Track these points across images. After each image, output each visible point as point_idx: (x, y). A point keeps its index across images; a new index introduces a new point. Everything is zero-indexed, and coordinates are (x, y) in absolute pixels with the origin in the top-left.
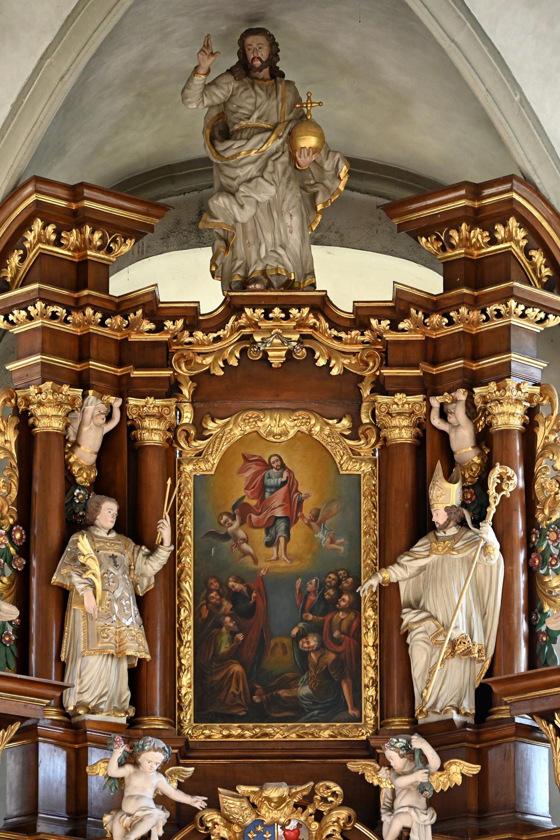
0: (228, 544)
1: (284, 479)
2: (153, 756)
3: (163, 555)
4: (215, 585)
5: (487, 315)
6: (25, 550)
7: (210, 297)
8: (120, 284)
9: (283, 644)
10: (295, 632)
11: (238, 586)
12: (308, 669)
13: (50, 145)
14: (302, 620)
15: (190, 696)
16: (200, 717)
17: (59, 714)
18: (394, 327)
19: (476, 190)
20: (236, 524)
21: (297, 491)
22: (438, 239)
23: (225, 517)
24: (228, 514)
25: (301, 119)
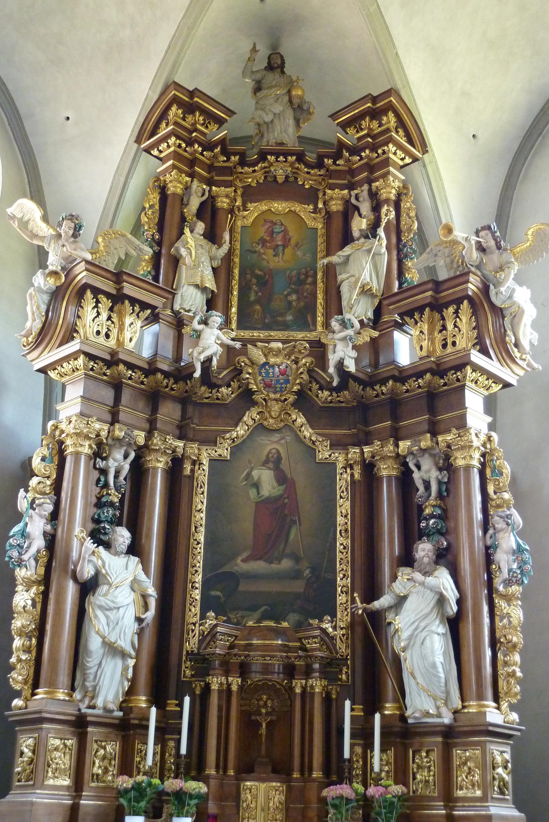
0: (255, 256)
1: (283, 229)
3: (225, 248)
4: (249, 272)
5: (378, 154)
9: (280, 298)
10: (285, 293)
11: (259, 273)
12: (291, 309)
14: (289, 287)
15: (235, 318)
17: (171, 312)
18: (334, 163)
19: (374, 99)
20: (260, 247)
21: (288, 234)
22: (355, 127)
23: (254, 244)
24: (256, 243)
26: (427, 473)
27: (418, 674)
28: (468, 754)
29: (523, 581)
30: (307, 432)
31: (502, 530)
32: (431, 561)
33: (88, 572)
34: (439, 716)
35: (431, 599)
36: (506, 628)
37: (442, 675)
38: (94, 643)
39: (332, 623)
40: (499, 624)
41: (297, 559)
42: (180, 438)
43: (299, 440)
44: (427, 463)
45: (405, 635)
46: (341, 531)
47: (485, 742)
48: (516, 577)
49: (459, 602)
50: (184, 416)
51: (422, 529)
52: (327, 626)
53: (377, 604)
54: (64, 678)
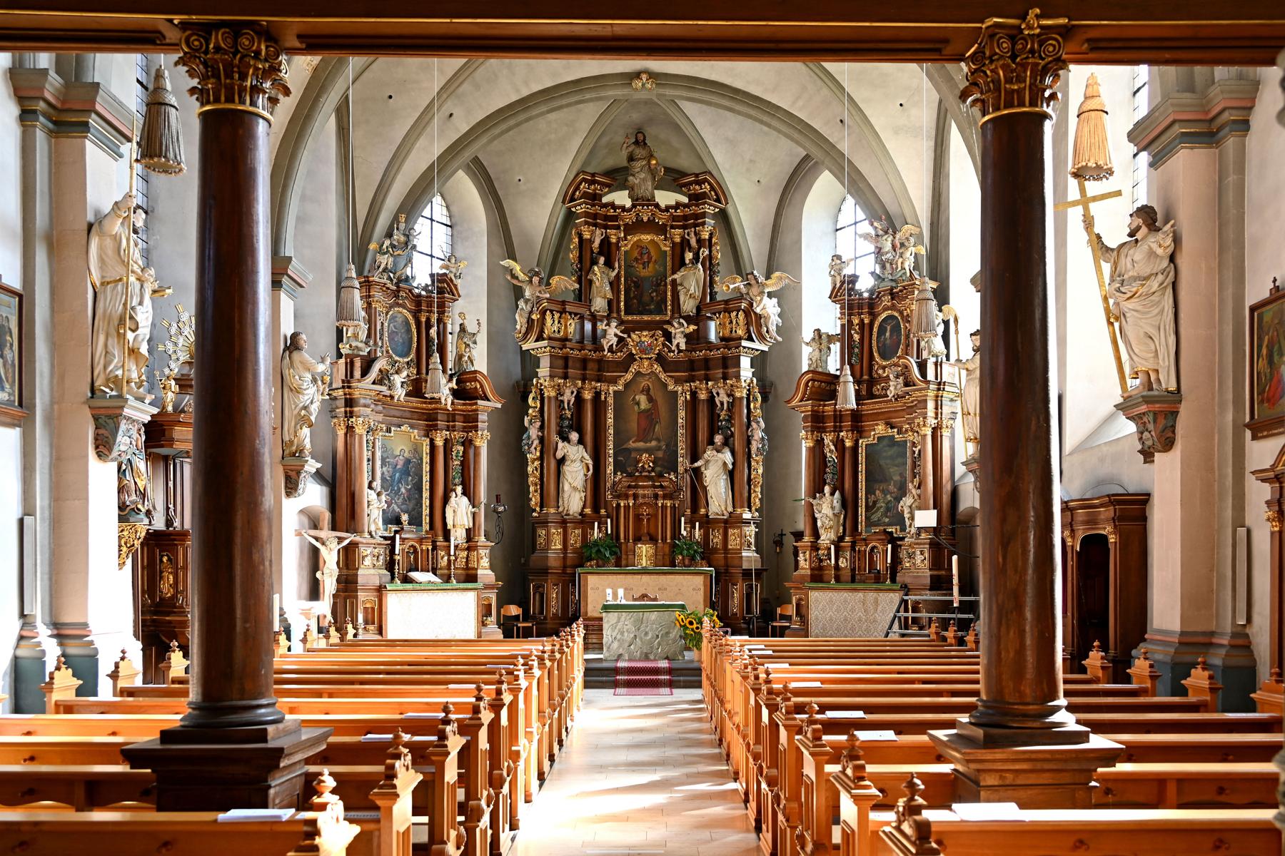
2: (614, 324)
6: (580, 270)
7: (628, 204)
8: (605, 200)
13: (586, 163)
16: (626, 313)
19: (697, 175)
25: (651, 156)
26: (723, 398)
30: (662, 376)
33: (559, 455)
35: (720, 463)
38: (567, 487)
40: (753, 473)
41: (658, 440)
42: (598, 381)
43: (660, 379)
44: (722, 392)
49: (733, 464)
50: (599, 370)
53: (696, 465)
54: (553, 503)
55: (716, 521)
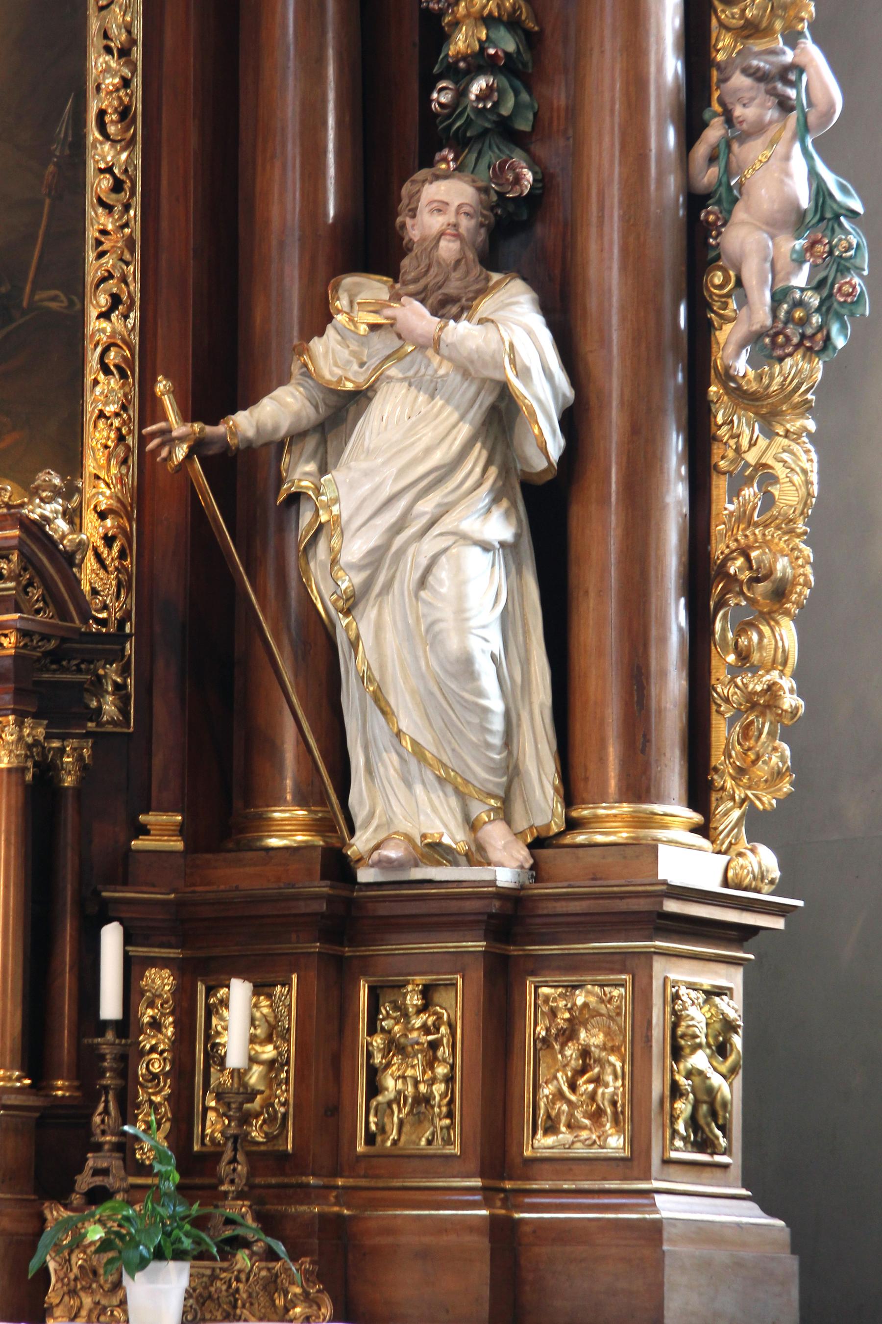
27: (401, 700)
28: (580, 999)
29: (828, 339)
31: (760, 128)
32: (471, 255)
34: (477, 855)
36: (750, 523)
37: (495, 703)
39: (68, 497)
40: (724, 506)
45: (355, 548)
46: (102, 113)
47: (648, 956)
48: (804, 322)
49: (572, 420)
51: (436, 115)
52: (48, 510)
53: (245, 423)
55: (420, 909)
